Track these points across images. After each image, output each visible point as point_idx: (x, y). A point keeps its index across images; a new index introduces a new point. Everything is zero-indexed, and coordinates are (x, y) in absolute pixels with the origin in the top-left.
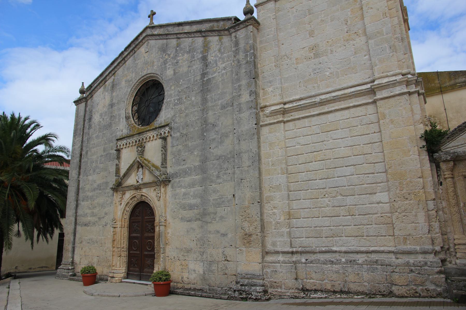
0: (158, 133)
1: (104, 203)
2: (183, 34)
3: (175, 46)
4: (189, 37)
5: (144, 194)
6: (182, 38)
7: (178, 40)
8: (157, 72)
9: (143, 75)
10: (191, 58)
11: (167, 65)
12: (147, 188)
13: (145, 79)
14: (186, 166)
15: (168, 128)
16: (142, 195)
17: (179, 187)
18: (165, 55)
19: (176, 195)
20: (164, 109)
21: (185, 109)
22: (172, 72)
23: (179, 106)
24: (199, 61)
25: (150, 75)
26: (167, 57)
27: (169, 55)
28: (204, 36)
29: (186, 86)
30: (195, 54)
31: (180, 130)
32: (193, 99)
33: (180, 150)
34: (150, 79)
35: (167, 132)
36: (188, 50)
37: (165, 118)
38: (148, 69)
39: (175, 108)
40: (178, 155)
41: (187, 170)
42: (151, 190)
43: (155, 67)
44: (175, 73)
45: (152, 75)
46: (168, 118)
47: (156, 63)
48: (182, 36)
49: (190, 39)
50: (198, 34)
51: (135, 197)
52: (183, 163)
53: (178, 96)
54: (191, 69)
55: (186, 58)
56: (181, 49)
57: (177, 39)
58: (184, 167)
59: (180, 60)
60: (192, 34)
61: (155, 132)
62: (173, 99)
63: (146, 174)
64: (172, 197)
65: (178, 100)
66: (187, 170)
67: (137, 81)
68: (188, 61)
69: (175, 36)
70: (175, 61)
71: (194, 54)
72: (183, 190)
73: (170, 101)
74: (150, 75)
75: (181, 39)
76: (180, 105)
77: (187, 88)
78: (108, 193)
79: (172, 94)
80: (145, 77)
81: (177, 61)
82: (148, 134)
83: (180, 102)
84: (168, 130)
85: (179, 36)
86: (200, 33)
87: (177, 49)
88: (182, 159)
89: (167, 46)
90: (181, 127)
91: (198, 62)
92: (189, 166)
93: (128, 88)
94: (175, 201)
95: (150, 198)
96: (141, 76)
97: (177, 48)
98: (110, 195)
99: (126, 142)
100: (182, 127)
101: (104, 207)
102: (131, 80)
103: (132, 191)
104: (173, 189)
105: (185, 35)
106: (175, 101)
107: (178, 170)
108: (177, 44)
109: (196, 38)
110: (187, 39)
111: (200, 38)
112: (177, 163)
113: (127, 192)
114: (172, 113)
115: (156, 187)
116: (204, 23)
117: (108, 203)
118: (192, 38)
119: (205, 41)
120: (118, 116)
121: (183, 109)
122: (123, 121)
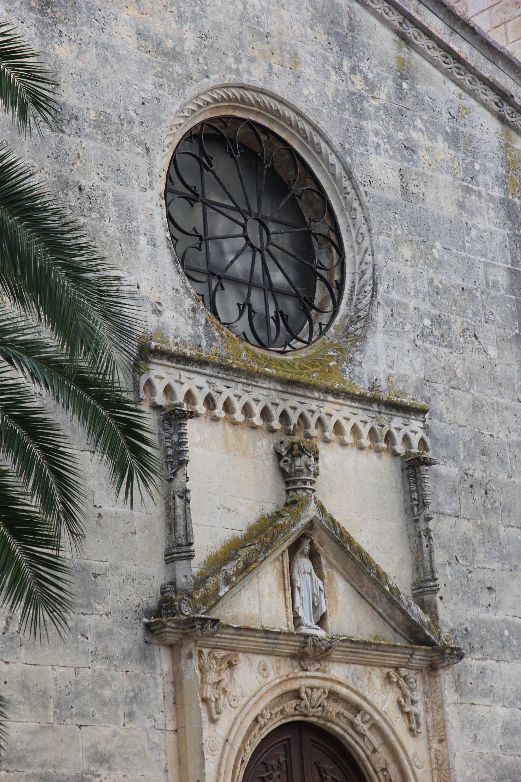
0: (377, 428)
1: (78, 695)
2: (431, 44)
3: (393, 62)
4: (447, 74)
5: (339, 688)
6: (422, 53)
7: (400, 49)
8: (322, 125)
9: (245, 80)
10: (466, 170)
11: (370, 125)
12: (353, 667)
13: (243, 100)
14: (500, 616)
15: (422, 425)
16: (333, 695)
17: (485, 695)
18: (354, 70)
19: (479, 728)
20: (380, 326)
21: (465, 375)
22: (394, 180)
23: (441, 349)
24: (494, 210)
25: (279, 106)
26: (359, 85)
27: (371, 86)
28: (502, 119)
29: (459, 281)
30: (477, 167)
31: (459, 455)
32: (492, 352)
33: (467, 542)
34: (260, 121)
35: (415, 440)
36: (448, 129)
37: (392, 372)
38: (271, 67)
39: (427, 350)
40: (465, 558)
41: (507, 633)
42: (370, 679)
43: (309, 90)
44: (405, 190)
45: (289, 113)
46: (404, 378)
47: (308, 72)
48: (423, 42)
49: (453, 87)
50: (491, 97)
51: (296, 694)
52: (485, 598)
53: (433, 305)
54: (469, 223)
55: (443, 156)
56: (419, 101)
57: (397, 39)
58: (490, 616)
59: (419, 146)
60: (469, 76)
61: (362, 415)
62: (412, 304)
63: (339, 598)
64: (462, 730)
65: (438, 321)
66: (507, 633)
67: (212, 89)
68: (454, 176)
69: (395, 18)
70: (401, 136)
71: (472, 164)
72: (500, 710)
73: (399, 303)
74: (279, 106)
75: (416, 56)
76: (447, 350)
77: (466, 294)
78: (99, 636)
79: (405, 280)
80: (249, 95)
81: (406, 140)
82: (328, 407)
83: (442, 336)
84: (421, 434)
85: (411, 32)
86: (496, 98)
87: (401, 85)
88: (481, 581)
89: (352, 28)
90: (461, 446)
91: (492, 213)
92: (510, 618)
93: (161, 86)
94: (477, 750)
95: (377, 717)
96: (231, 78)
97: (402, 77)
98: (115, 650)
99: (207, 390)
100: (465, 445)
101: (83, 716)
102: (174, 49)
103: (270, 661)
104: (461, 695)
105: (437, 54)
106: (421, 318)
107: (472, 621)
108: (401, 62)
109: (473, 102)
110: (440, 76)
111: (488, 114)
112: (465, 593)
113: (241, 656)
114: (417, 366)
115: (404, 672)
116: (500, 63)
117: (107, 693)
118: (460, 91)
119: (507, 145)
120: (113, 211)
121: (459, 373)
122: (154, 258)
